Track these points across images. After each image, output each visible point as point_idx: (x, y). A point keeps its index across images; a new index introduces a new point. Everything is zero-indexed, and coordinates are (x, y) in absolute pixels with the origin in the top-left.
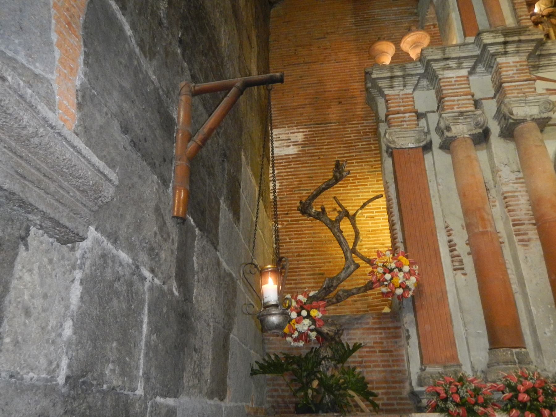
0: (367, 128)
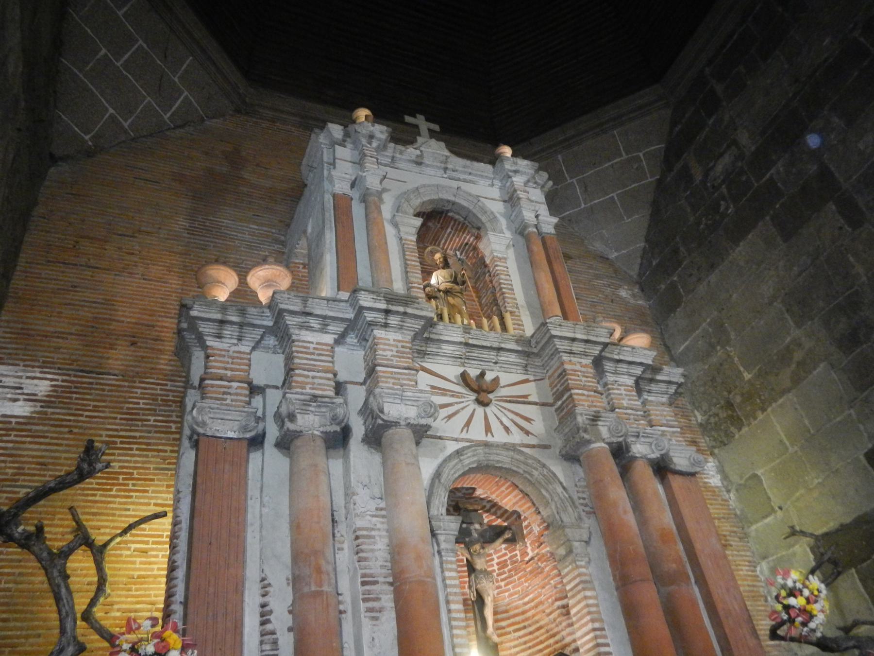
0: (171, 394)
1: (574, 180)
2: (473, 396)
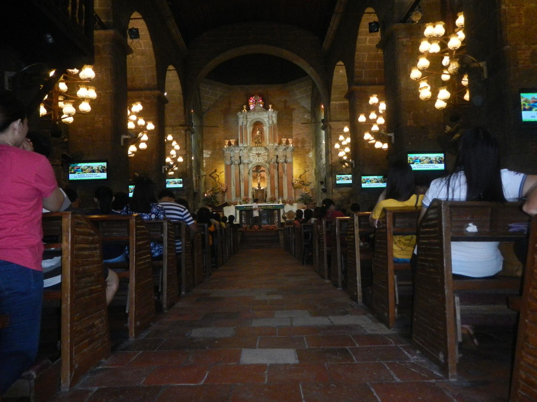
2: (257, 156)
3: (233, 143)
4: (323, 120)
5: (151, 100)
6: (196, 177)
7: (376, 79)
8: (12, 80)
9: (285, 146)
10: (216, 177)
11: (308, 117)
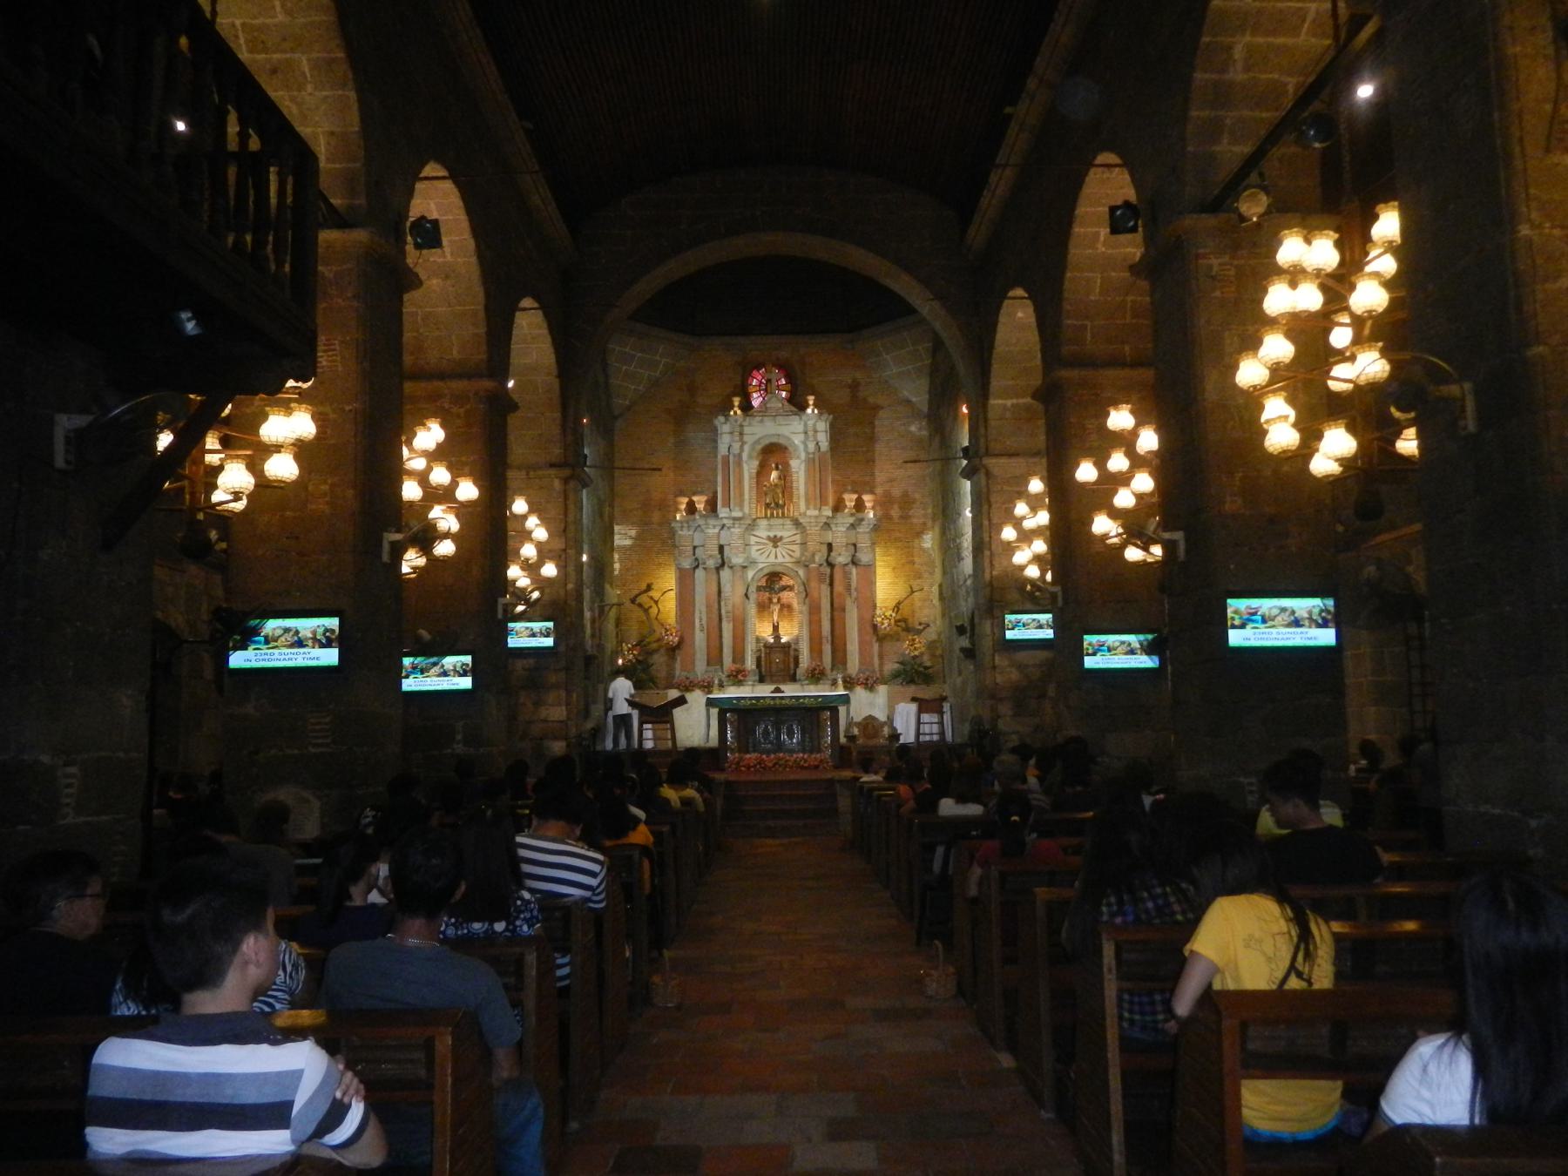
1: (888, 357)
3: (700, 506)
4: (966, 450)
5: (468, 407)
6: (592, 609)
7: (1127, 348)
8: (77, 439)
9: (852, 515)
10: (651, 607)
11: (920, 429)
